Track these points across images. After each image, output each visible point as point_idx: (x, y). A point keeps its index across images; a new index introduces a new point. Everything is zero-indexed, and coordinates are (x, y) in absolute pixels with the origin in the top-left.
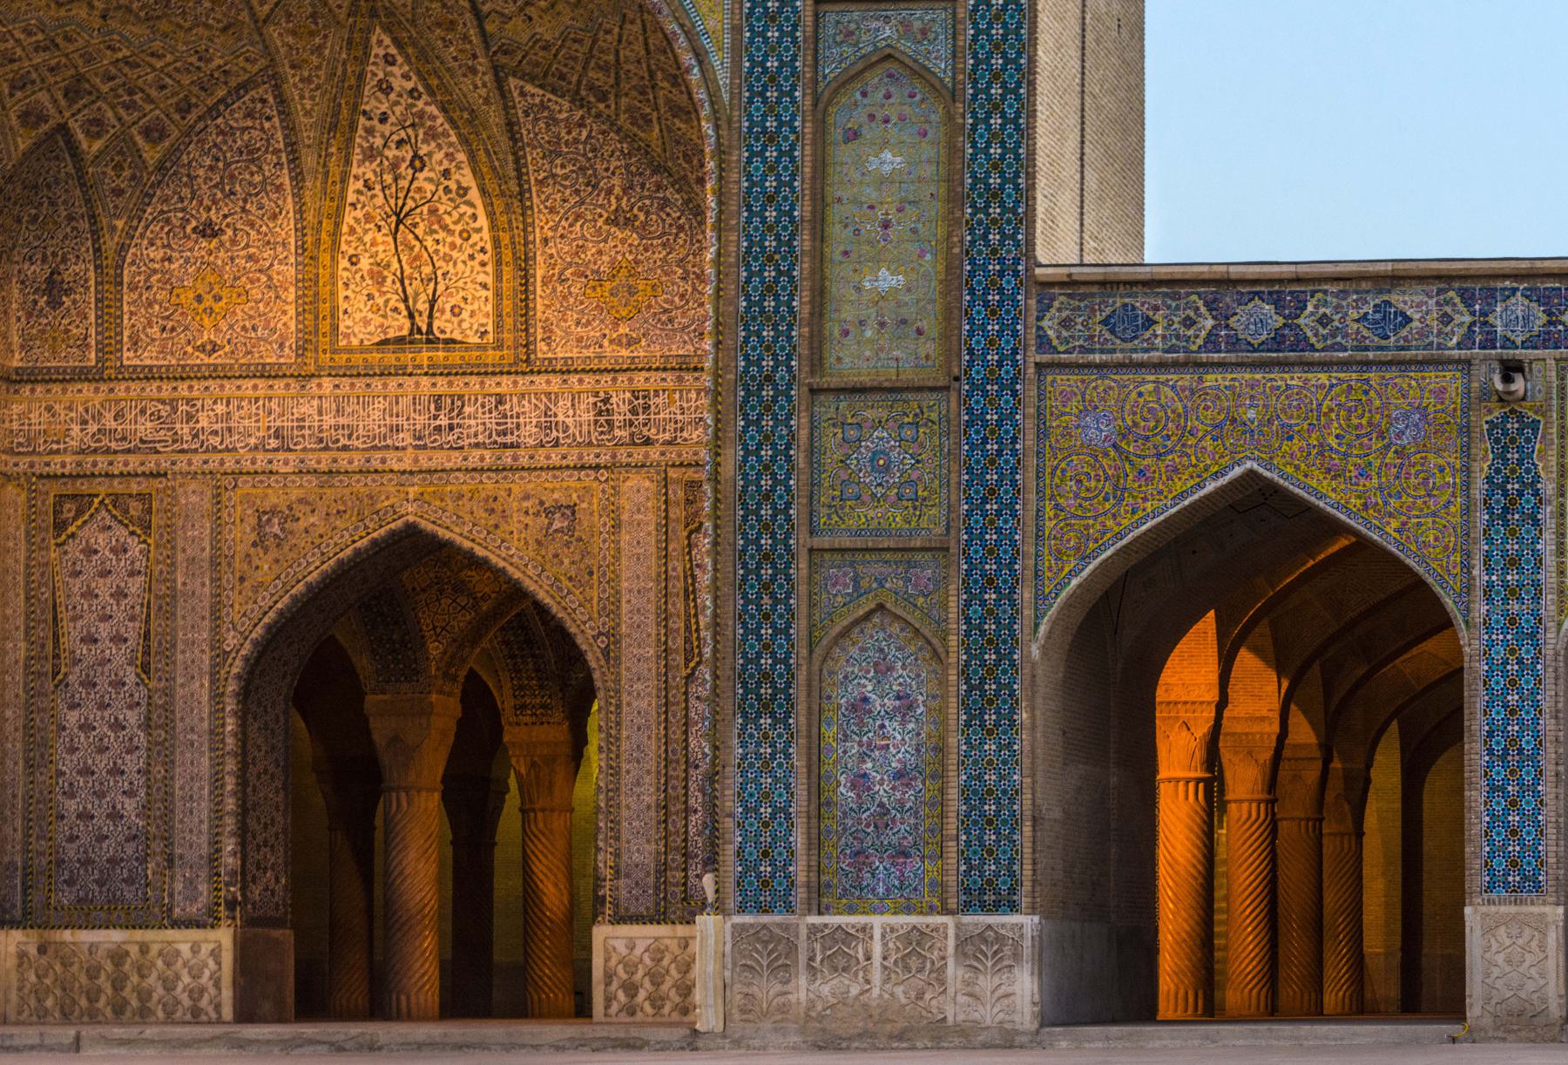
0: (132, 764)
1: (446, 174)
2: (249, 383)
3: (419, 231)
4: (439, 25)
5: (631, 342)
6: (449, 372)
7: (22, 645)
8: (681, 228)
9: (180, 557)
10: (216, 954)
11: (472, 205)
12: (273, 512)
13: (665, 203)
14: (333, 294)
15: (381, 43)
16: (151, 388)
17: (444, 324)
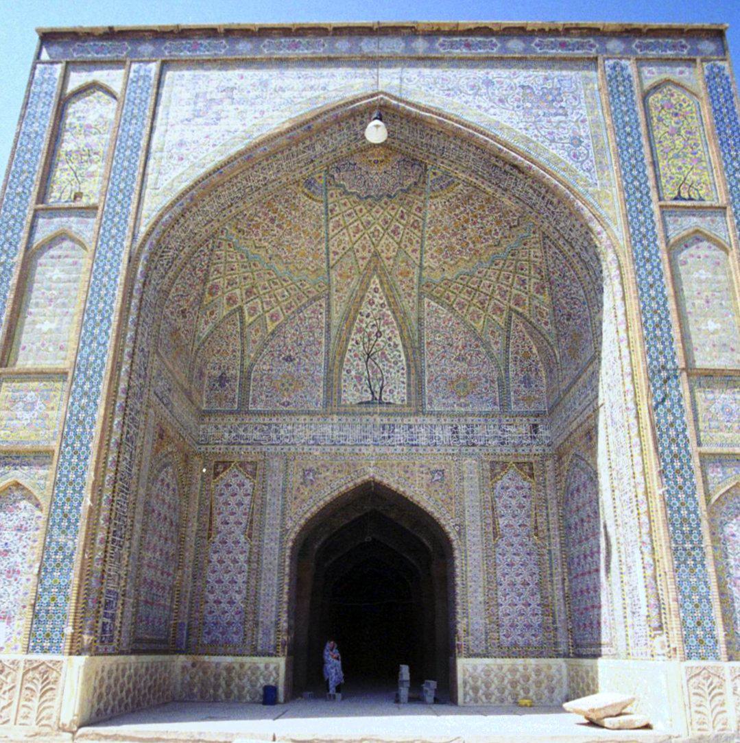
0: (240, 579)
1: (390, 339)
2: (303, 417)
3: (377, 361)
4: (401, 274)
5: (466, 405)
6: (388, 414)
7: (195, 524)
8: (485, 363)
9: (269, 488)
10: (277, 669)
11: (398, 351)
12: (310, 470)
13: (478, 353)
14: (339, 385)
15: (375, 282)
16: (260, 420)
17: (386, 397)
